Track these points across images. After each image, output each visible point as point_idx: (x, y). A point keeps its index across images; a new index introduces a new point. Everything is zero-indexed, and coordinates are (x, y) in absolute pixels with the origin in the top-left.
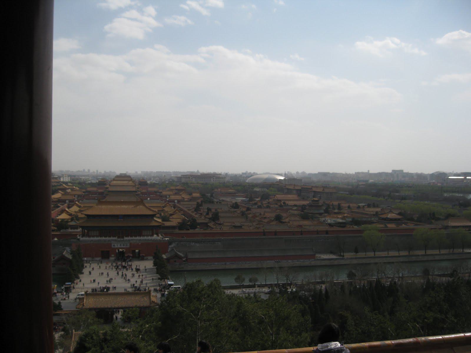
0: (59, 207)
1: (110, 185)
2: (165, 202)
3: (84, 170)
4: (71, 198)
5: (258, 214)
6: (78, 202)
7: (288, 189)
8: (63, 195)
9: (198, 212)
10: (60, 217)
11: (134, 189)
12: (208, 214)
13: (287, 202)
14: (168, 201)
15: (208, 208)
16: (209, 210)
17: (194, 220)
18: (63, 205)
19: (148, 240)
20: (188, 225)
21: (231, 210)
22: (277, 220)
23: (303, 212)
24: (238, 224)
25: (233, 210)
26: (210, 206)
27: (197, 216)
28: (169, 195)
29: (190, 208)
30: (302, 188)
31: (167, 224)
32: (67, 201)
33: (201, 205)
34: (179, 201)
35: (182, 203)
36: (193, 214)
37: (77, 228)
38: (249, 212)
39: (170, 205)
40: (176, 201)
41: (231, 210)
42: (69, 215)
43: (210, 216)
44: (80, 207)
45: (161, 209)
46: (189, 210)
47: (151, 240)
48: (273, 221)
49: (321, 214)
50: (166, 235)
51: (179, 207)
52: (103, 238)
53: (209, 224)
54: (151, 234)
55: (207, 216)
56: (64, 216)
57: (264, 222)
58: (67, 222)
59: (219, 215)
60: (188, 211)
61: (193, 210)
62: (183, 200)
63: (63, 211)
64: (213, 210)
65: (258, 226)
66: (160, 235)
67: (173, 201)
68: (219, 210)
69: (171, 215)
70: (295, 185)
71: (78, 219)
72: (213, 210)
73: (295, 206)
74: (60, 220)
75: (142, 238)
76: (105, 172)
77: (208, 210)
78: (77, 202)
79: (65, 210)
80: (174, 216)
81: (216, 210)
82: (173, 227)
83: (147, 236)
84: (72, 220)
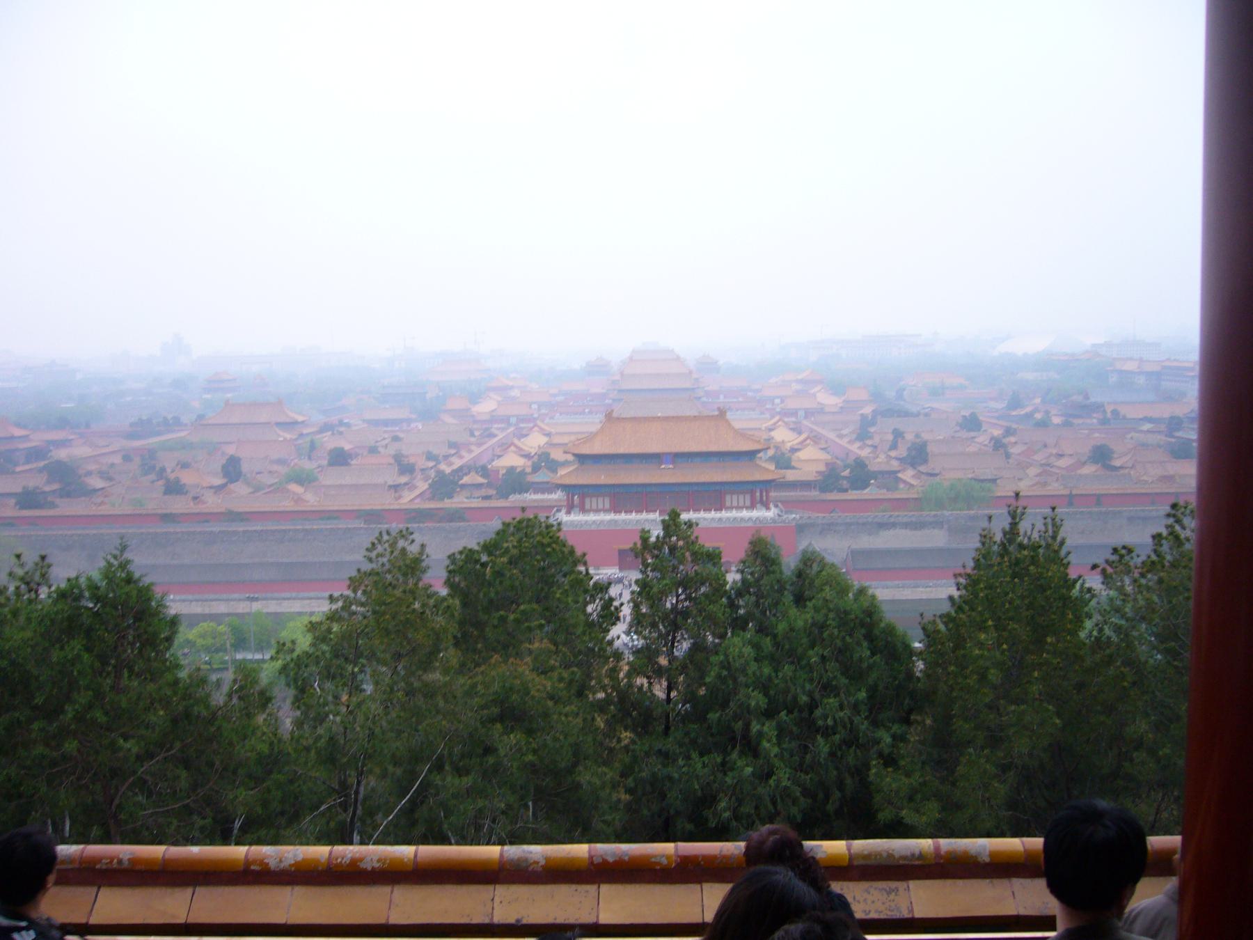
0: (495, 436)
2: (772, 417)
6: (543, 421)
7: (1121, 372)
9: (869, 442)
10: (498, 463)
12: (894, 446)
14: (779, 413)
16: (898, 434)
17: (860, 464)
18: (503, 429)
19: (742, 519)
20: (845, 478)
21: (959, 434)
22: (1096, 462)
23: (1173, 437)
29: (844, 432)
30: (1164, 367)
31: (790, 476)
32: (513, 420)
33: (873, 423)
34: (808, 413)
36: (855, 448)
37: (550, 491)
38: (1013, 439)
39: (786, 424)
40: (801, 413)
41: (959, 434)
43: (902, 451)
44: (548, 435)
46: (841, 436)
47: (750, 519)
48: (1084, 463)
50: (788, 505)
51: (812, 431)
52: (623, 516)
53: (900, 475)
54: (748, 503)
55: (893, 454)
56: (512, 460)
57: (1059, 468)
58: (523, 473)
59: (930, 448)
60: (837, 440)
61: (854, 436)
64: (909, 437)
66: (771, 505)
67: (794, 413)
68: (926, 436)
69: (794, 450)
70: (1141, 360)
71: (553, 466)
72: (909, 437)
74: (503, 472)
75: (724, 514)
77: (895, 437)
78: (539, 423)
79: (512, 444)
80: (802, 455)
81: (917, 436)
82: (806, 485)
83: (739, 508)
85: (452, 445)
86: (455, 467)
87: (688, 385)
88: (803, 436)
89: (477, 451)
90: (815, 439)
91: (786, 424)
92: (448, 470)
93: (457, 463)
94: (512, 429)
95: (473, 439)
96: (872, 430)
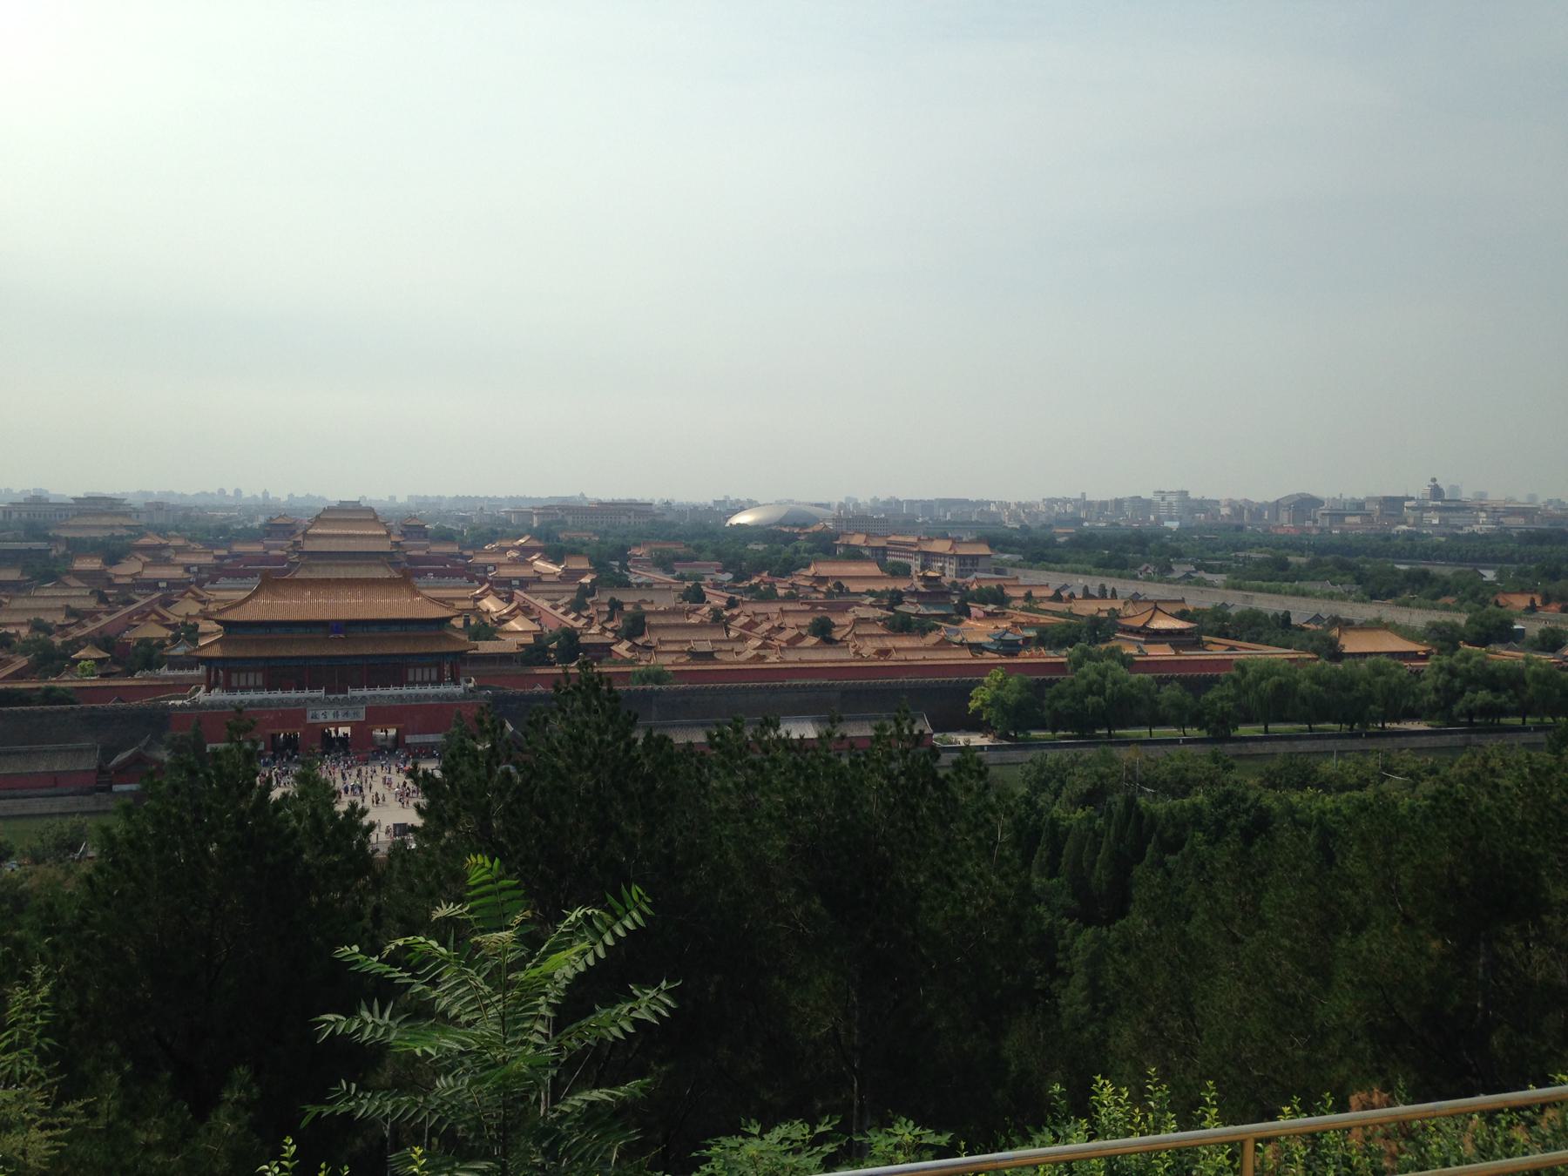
0: (134, 602)
1: (305, 534)
3: (222, 491)
4: (178, 573)
5: (758, 620)
8: (145, 565)
9: (585, 613)
11: (385, 546)
13: (845, 584)
15: (612, 599)
16: (616, 606)
18: (146, 595)
24: (706, 647)
25: (687, 605)
26: (621, 596)
27: (580, 623)
28: (496, 566)
34: (524, 583)
35: (535, 587)
38: (735, 611)
40: (516, 582)
42: (169, 627)
44: (203, 602)
45: (469, 605)
49: (945, 618)
55: (609, 626)
56: (155, 632)
62: (538, 579)
63: (143, 615)
64: (628, 608)
65: (762, 652)
67: (507, 582)
73: (871, 593)
76: (291, 496)
84: (175, 639)
85: (71, 612)
86: (69, 638)
87: (387, 549)
88: (514, 605)
89: (105, 619)
90: (526, 610)
91: (497, 594)
92: (58, 641)
93: (77, 633)
94: (158, 594)
95: (103, 607)
96: (589, 601)
